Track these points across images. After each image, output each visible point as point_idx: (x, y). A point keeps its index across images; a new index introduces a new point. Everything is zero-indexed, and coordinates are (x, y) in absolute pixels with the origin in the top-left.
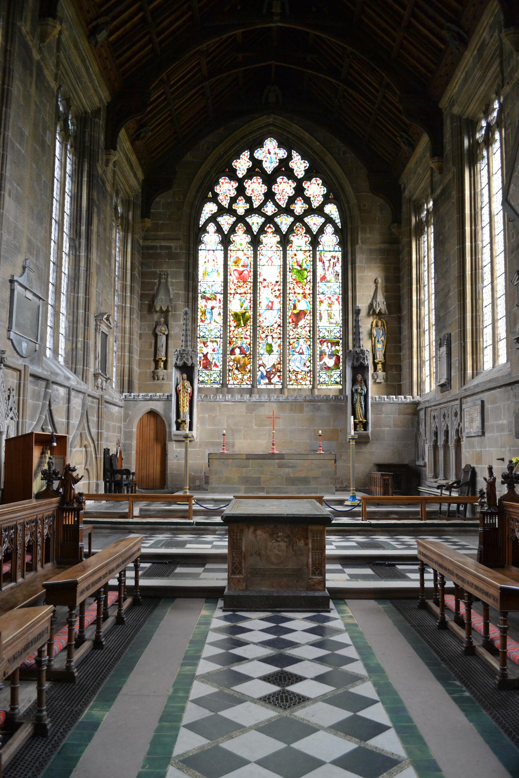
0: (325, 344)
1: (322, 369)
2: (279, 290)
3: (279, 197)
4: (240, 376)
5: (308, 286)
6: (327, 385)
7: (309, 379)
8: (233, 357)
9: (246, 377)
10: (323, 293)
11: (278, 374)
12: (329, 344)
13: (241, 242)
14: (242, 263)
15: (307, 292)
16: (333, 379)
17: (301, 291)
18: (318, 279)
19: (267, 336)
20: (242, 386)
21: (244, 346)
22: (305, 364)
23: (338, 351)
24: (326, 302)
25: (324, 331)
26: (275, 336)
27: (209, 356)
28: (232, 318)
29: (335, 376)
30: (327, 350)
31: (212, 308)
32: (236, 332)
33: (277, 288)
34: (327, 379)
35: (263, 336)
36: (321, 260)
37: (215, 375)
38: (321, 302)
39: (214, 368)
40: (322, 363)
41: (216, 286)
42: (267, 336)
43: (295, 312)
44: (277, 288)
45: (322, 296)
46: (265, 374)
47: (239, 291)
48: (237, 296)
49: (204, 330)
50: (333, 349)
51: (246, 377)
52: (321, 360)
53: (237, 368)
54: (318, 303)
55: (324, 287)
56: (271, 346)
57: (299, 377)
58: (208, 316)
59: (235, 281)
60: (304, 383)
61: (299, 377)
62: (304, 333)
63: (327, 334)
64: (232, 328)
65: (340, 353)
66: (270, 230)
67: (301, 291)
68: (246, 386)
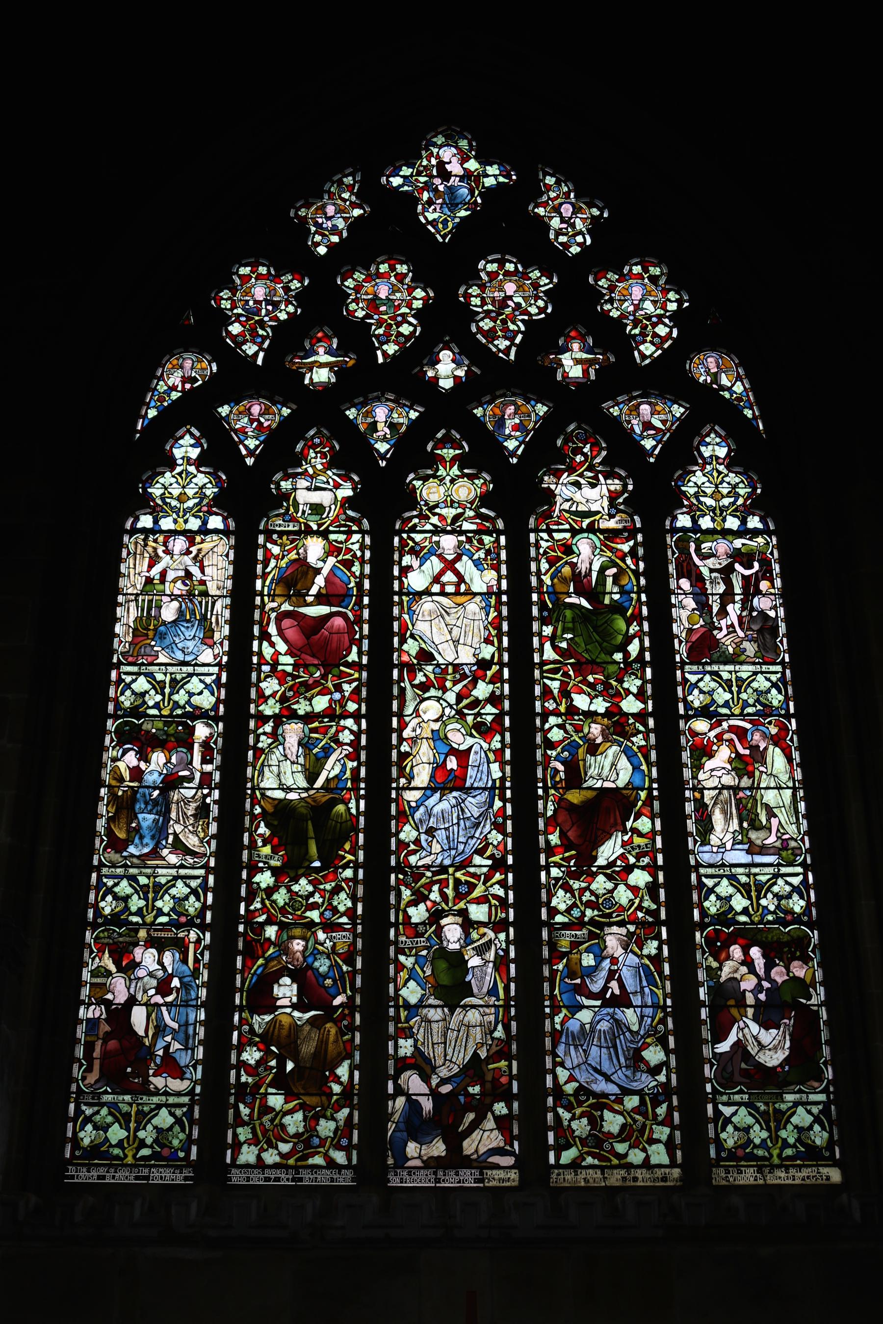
0: (736, 951)
1: (726, 1080)
2: (494, 700)
3: (487, 324)
4: (295, 1123)
5: (633, 684)
6: (763, 1165)
7: (661, 1133)
8: (260, 1021)
9: (326, 1128)
10: (705, 712)
11: (500, 1108)
12: (755, 952)
13: (324, 498)
14: (320, 581)
15: (631, 705)
16: (788, 1134)
17: (600, 705)
18: (682, 650)
19: (436, 916)
20: (308, 1179)
21: (322, 965)
22: (636, 1060)
23: (802, 986)
24: (724, 753)
25: (725, 888)
26: (478, 913)
27: (139, 1017)
28: (263, 829)
29: (802, 1117)
30: (748, 984)
31: (171, 782)
32: (281, 897)
33: (482, 690)
34: (758, 1134)
35: (418, 914)
36: (688, 570)
37: (164, 1119)
38: (703, 751)
39: (158, 1082)
40: (724, 1047)
41: (195, 685)
42: (436, 916)
43: (574, 797)
44: (482, 690)
45: (701, 725)
46: (427, 1105)
47: (302, 708)
48: (293, 732)
49: (124, 888)
50: (779, 974)
51: (326, 1128)
52: (720, 1036)
53: (281, 1082)
54: (686, 756)
55: (708, 683)
56: (457, 960)
57: (613, 1122)
58: (147, 819)
59: (287, 662)
60: (636, 1157)
61: (613, 1122)
62: (623, 895)
63: (739, 903)
64: (265, 879)
65: (818, 996)
66: (448, 453)
67: (600, 705)
68: (324, 1178)
